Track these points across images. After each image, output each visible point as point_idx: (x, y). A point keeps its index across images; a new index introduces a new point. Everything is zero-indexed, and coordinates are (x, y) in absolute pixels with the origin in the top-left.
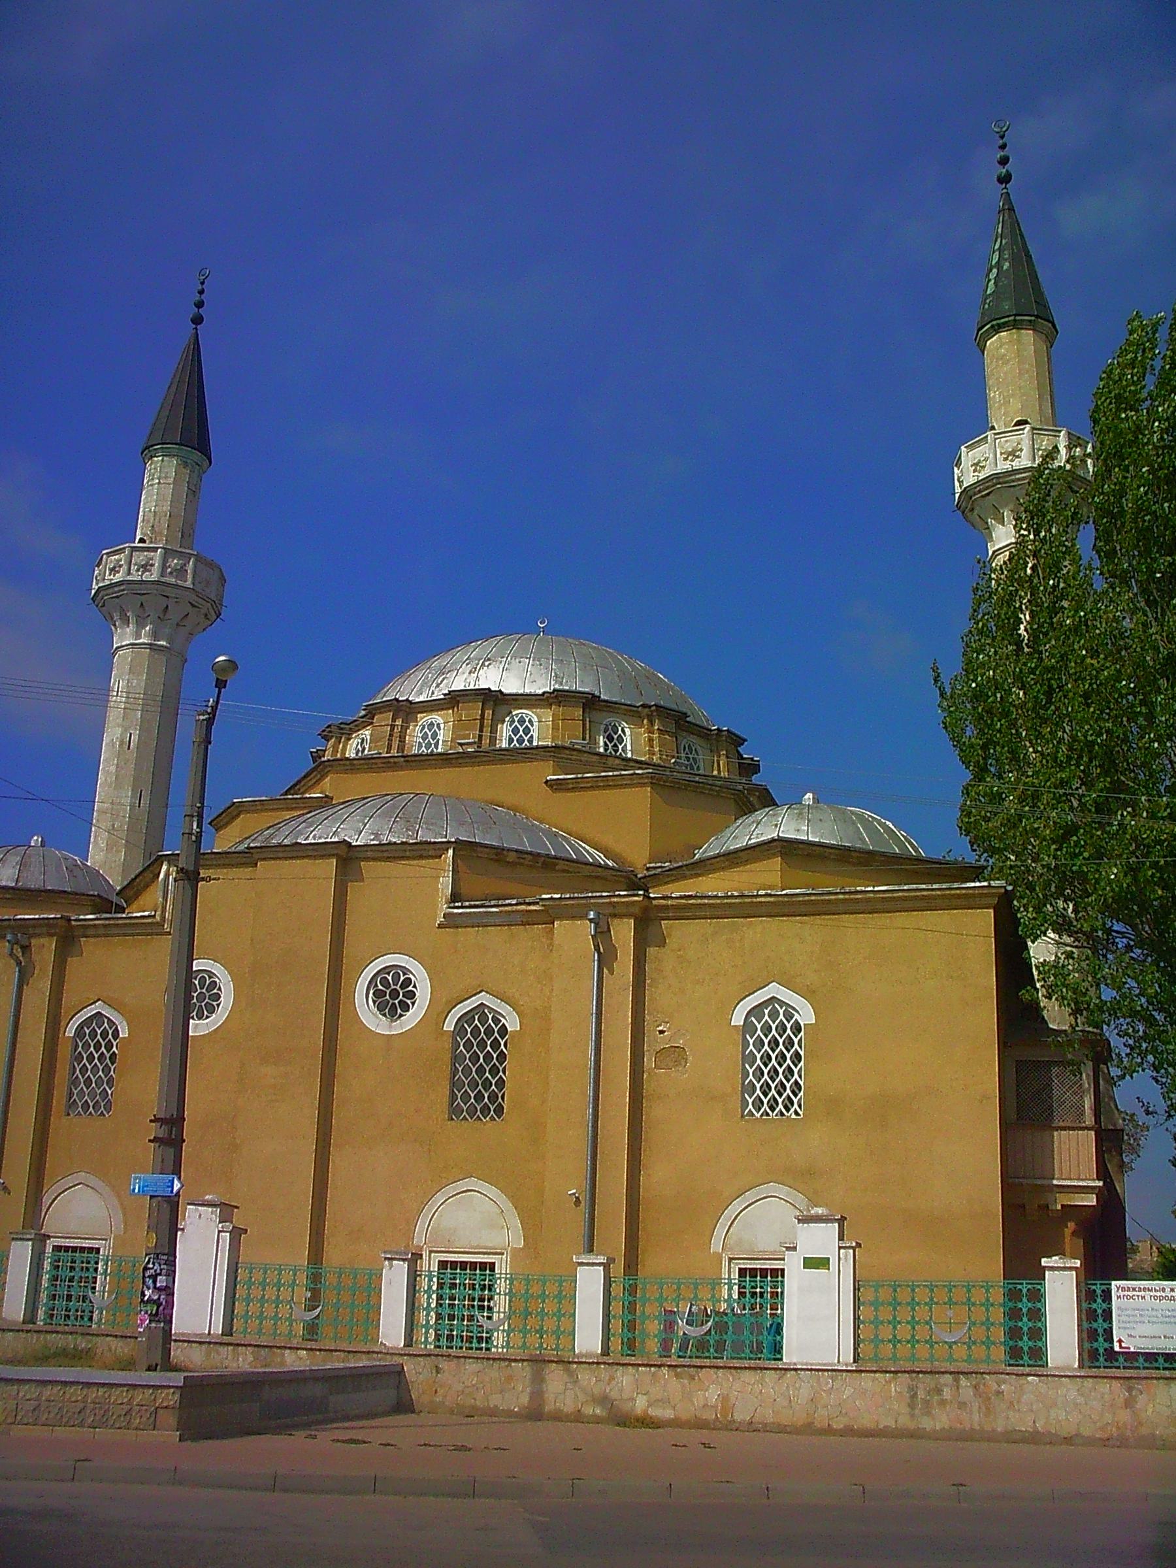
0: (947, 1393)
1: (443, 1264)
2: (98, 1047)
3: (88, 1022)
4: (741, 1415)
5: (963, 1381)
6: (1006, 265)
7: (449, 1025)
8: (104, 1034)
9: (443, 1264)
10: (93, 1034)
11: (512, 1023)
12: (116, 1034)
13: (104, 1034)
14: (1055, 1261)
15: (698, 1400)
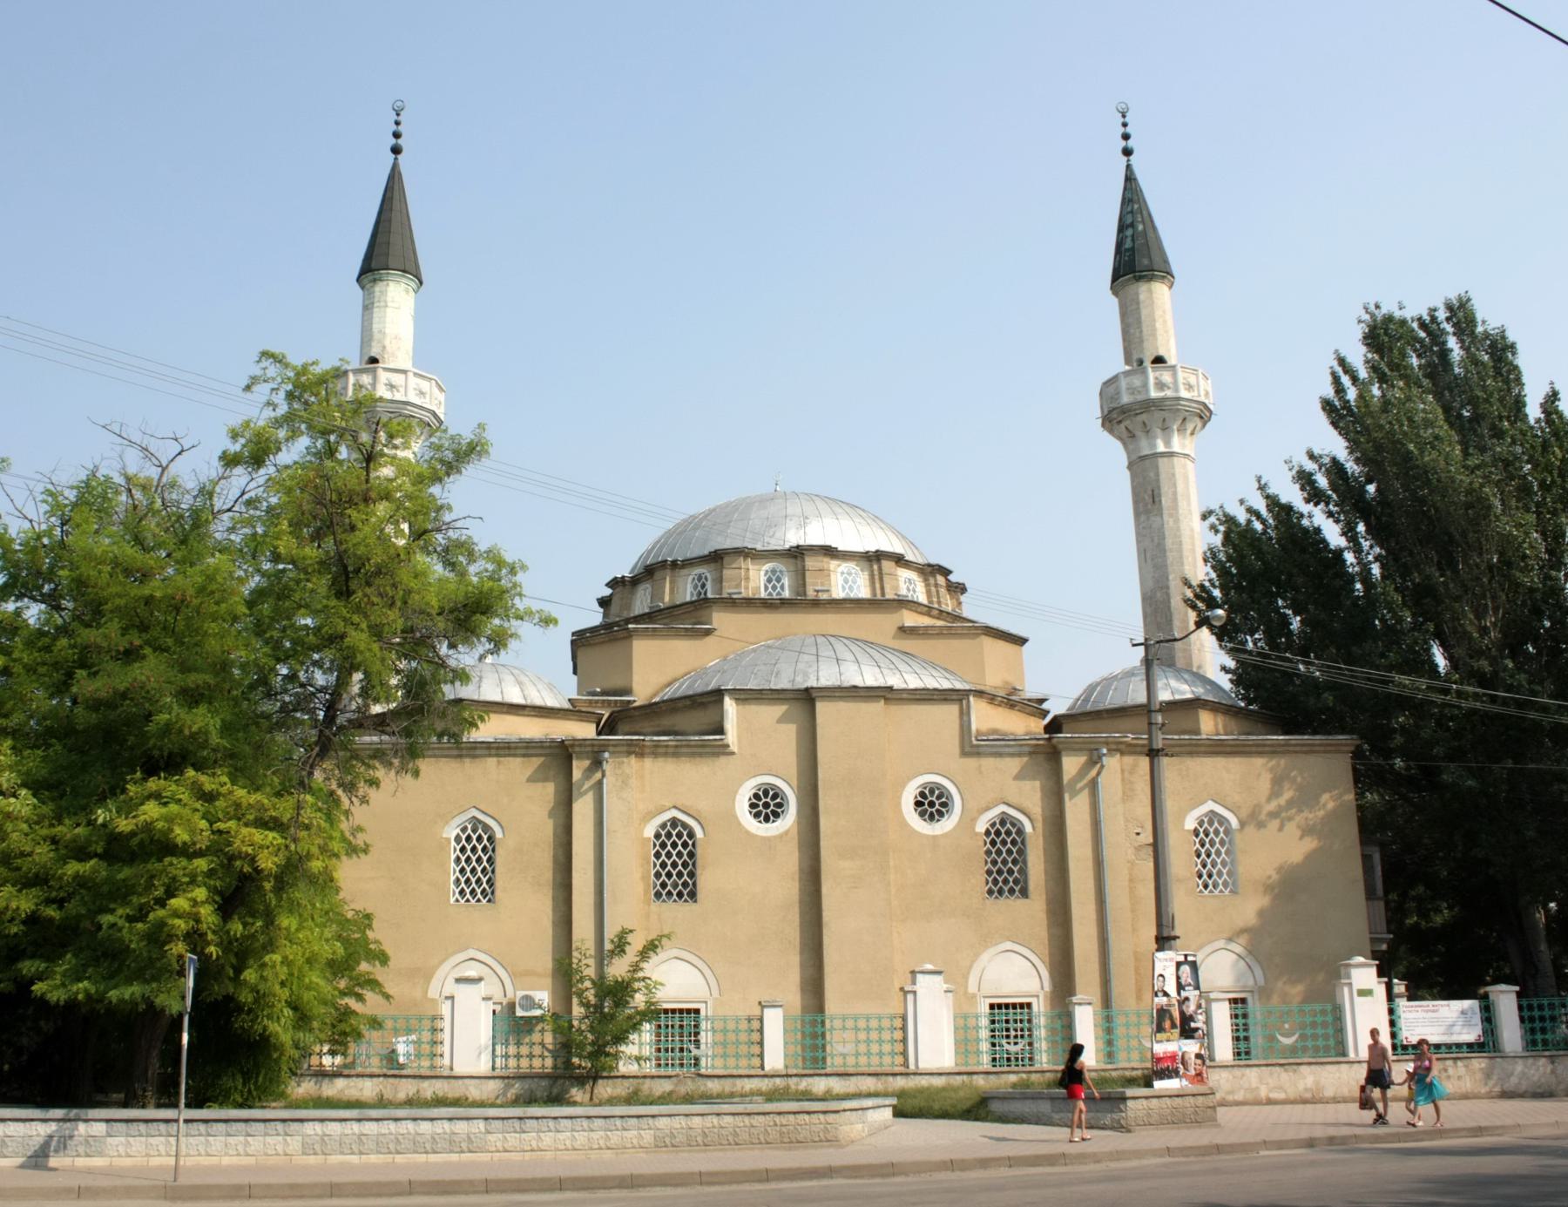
0: (1451, 1071)
1: (992, 1006)
2: (674, 845)
3: (663, 826)
4: (1329, 1093)
5: (1459, 1063)
6: (1140, 227)
7: (981, 827)
8: (679, 835)
9: (992, 1006)
10: (669, 835)
11: (1028, 828)
12: (691, 835)
13: (679, 835)
14: (1503, 987)
15: (1301, 1087)
